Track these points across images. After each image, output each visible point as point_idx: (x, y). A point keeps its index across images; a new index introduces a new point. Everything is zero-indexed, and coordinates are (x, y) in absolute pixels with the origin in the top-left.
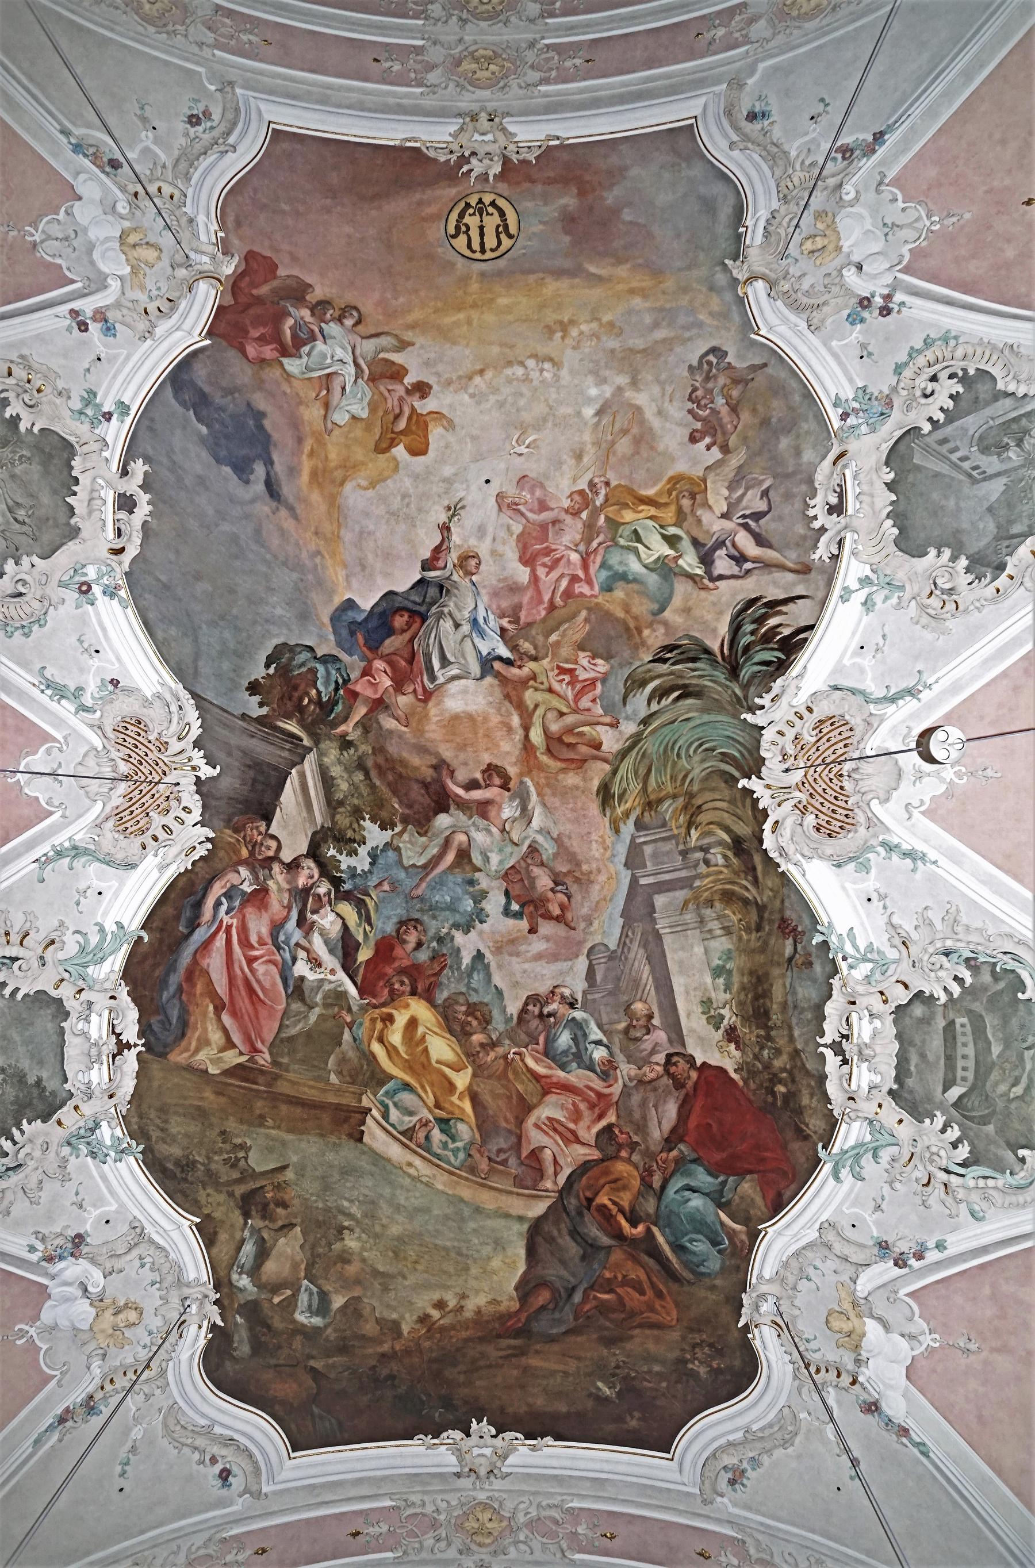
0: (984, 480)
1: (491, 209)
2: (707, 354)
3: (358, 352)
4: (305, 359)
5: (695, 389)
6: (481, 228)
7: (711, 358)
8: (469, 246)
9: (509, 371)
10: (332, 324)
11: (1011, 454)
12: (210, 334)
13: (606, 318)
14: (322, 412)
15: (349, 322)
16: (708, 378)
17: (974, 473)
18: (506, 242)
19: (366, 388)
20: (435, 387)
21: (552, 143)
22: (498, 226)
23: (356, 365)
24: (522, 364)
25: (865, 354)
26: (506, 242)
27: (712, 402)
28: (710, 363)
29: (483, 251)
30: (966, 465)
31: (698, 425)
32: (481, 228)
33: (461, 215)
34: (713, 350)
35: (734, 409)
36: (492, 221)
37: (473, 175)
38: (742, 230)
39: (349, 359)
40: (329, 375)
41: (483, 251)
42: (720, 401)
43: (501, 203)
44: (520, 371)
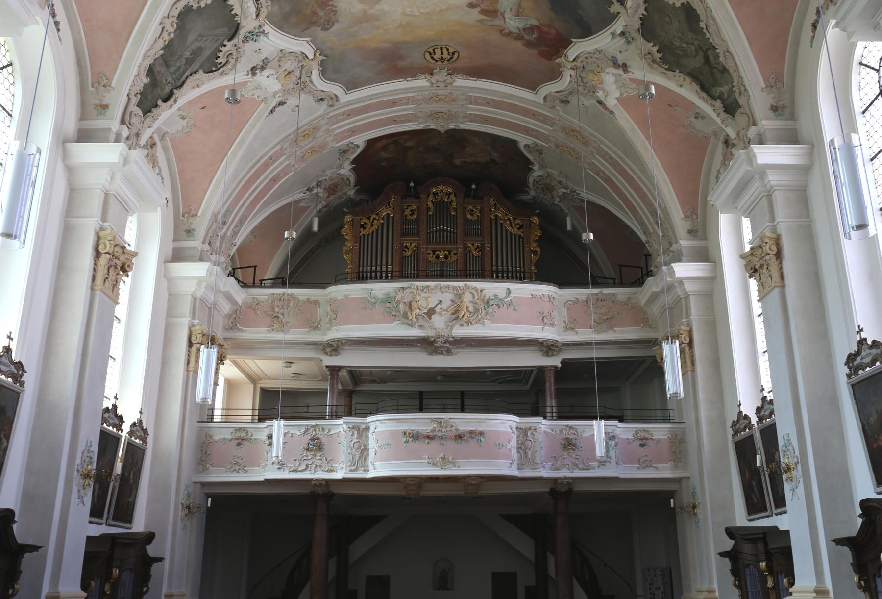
0: (196, 39)
1: (438, 60)
2: (330, 28)
3: (503, 22)
4: (529, 23)
5: (334, 15)
6: (442, 53)
7: (328, 27)
8: (448, 50)
9: (428, 10)
10: (515, 32)
11: (189, 53)
12: (572, 42)
13: (381, 31)
14: (522, 4)
15: (506, 31)
16: (329, 20)
17: (200, 38)
18: (431, 50)
19: (500, 9)
20: (465, 6)
21: (410, 79)
22: (435, 54)
23: (504, 18)
24: (421, 13)
25: (258, 51)
26: (431, 50)
27: (325, 13)
28: (328, 25)
29: (441, 49)
30: (205, 39)
31: (331, 3)
32: (442, 53)
33: (451, 58)
34: (328, 29)
35: (314, 13)
36: (438, 55)
37: (446, 69)
38: (321, 69)
39: (507, 20)
40: (518, 16)
41: (441, 49)
42: (322, 14)
43: (434, 62)
44: (422, 11)
